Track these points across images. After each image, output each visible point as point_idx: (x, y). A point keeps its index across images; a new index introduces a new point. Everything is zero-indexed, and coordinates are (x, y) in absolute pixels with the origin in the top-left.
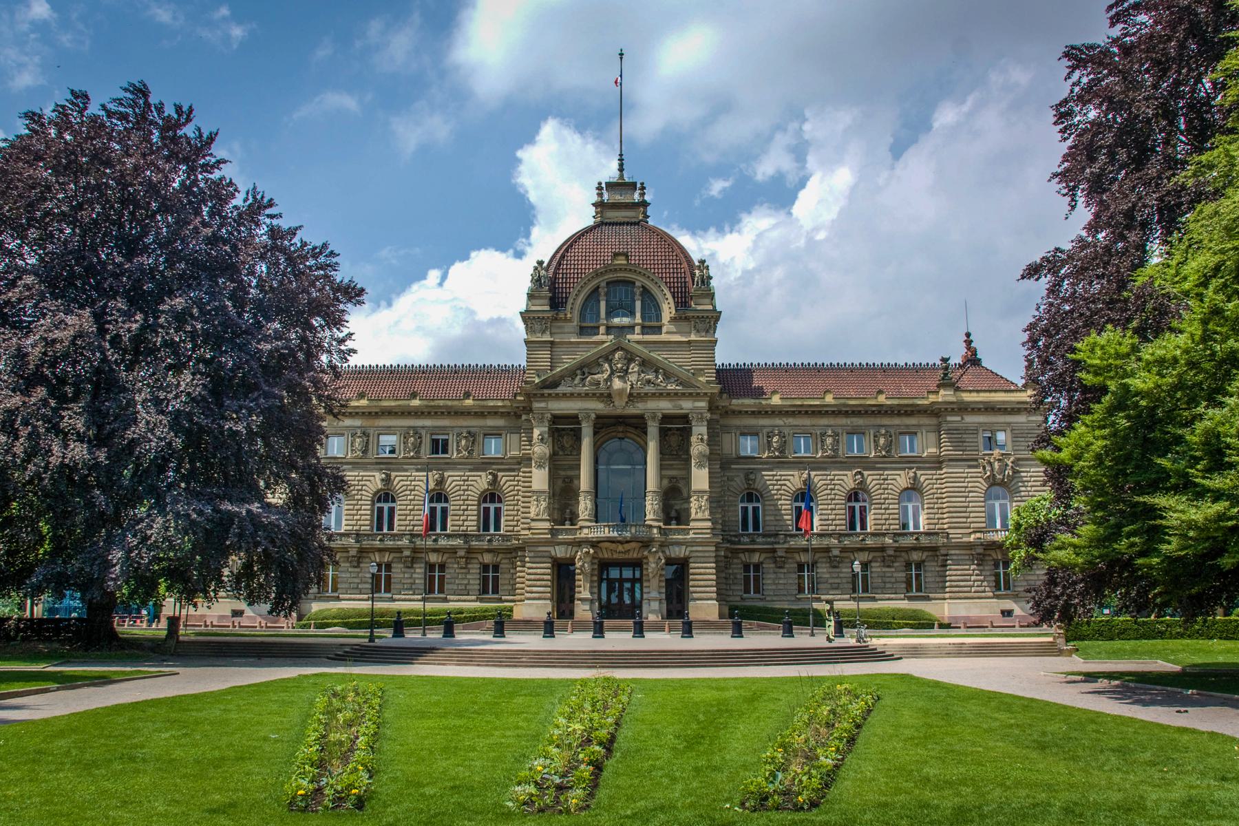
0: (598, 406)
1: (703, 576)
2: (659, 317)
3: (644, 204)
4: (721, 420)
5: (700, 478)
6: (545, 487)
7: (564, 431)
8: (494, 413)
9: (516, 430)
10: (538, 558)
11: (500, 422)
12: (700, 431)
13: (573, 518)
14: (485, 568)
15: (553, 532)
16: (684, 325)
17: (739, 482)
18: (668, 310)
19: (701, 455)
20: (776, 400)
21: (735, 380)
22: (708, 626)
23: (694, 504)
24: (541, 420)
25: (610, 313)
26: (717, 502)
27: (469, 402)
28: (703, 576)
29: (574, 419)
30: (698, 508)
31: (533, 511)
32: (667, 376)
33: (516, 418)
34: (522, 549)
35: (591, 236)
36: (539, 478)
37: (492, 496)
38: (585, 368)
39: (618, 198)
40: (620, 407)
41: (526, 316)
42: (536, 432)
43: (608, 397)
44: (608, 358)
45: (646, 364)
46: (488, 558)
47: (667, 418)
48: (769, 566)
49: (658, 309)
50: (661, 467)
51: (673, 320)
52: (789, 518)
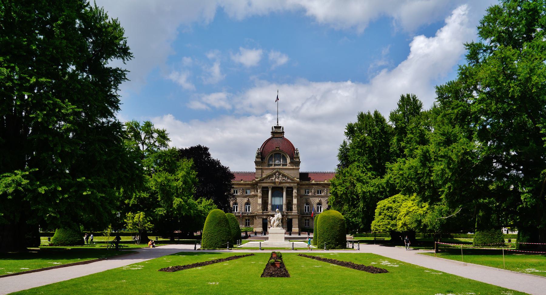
0: (273, 185)
1: (295, 222)
2: (286, 162)
3: (283, 132)
4: (299, 186)
5: (295, 201)
6: (261, 203)
7: (265, 191)
8: (248, 184)
9: (254, 188)
10: (259, 218)
11: (249, 186)
12: (295, 191)
13: (267, 209)
14: (246, 220)
15: (262, 213)
16: (292, 164)
17: (304, 201)
18: (288, 160)
19: (295, 196)
20: (313, 182)
21: (304, 176)
22: (295, 233)
23: (293, 207)
24: (260, 188)
25: (275, 161)
26: (299, 205)
27: (242, 182)
28: (295, 222)
29: (267, 188)
30: (295, 208)
31: (258, 208)
32: (288, 178)
33: (254, 186)
34: (256, 216)
35: (270, 141)
36: (260, 201)
37: (248, 203)
38: (269, 177)
39: (278, 131)
40: (277, 185)
41: (256, 163)
42: (259, 190)
43: (275, 183)
44: (275, 174)
45: (284, 176)
46: (247, 218)
47: (288, 188)
48: (311, 220)
49: (286, 160)
50: (287, 197)
51: (290, 163)
52: (316, 209)
